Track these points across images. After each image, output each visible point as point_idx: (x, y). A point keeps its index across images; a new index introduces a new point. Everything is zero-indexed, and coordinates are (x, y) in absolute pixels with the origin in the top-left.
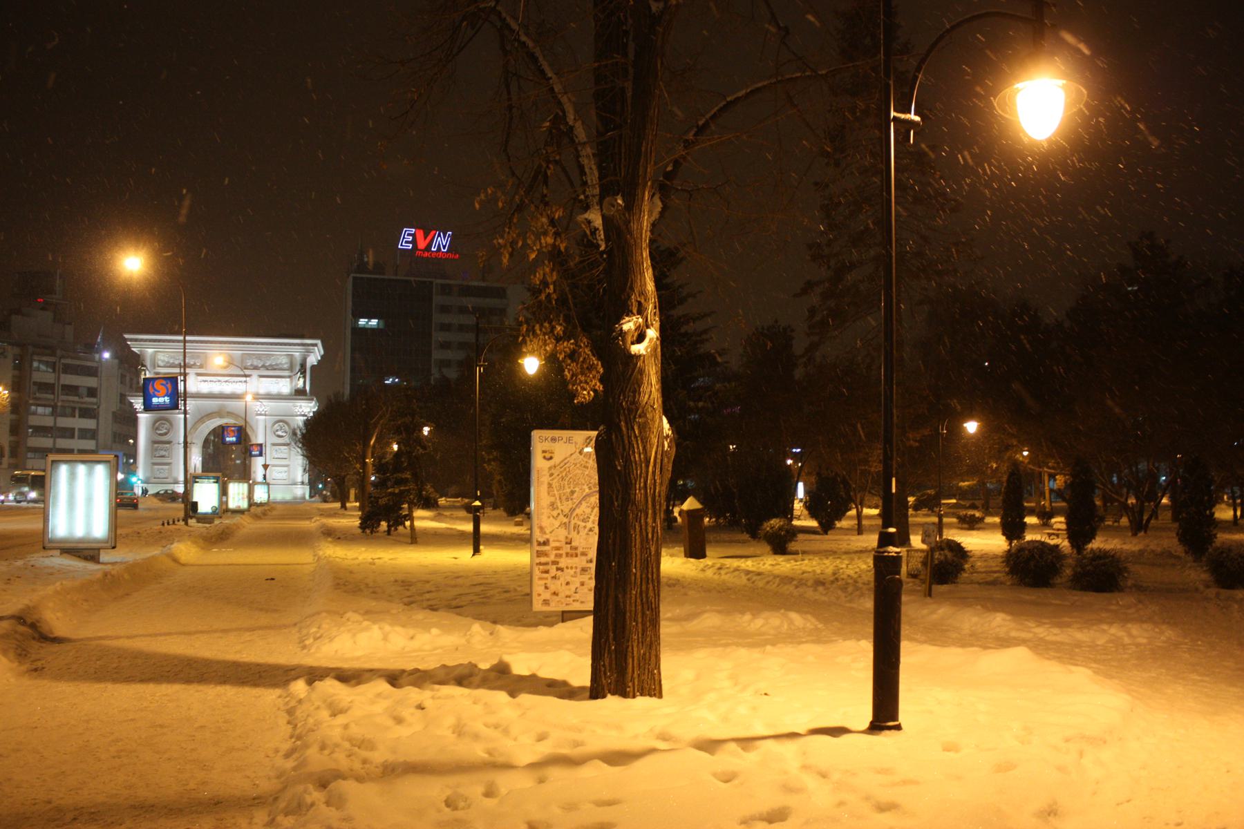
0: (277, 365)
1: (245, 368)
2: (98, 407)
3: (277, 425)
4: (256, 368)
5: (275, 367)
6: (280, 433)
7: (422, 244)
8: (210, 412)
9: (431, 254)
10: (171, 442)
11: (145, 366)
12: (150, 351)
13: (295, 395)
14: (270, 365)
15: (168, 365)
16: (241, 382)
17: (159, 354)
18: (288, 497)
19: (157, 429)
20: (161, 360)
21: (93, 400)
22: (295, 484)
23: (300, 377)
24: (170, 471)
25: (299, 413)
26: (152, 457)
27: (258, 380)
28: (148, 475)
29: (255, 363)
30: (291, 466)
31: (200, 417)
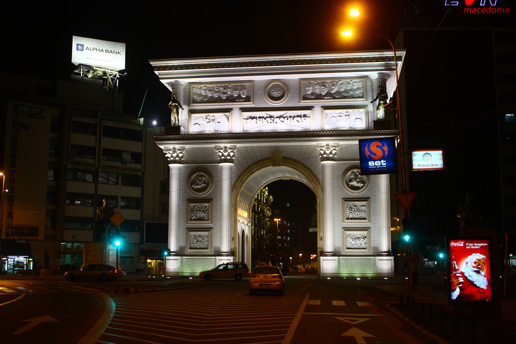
0: (346, 91)
1: (305, 98)
2: (143, 174)
3: (350, 173)
4: (319, 97)
5: (345, 95)
6: (354, 183)
8: (260, 158)
9: (480, 11)
10: (212, 199)
11: (177, 102)
12: (184, 82)
13: (375, 129)
14: (338, 93)
15: (207, 99)
16: (298, 116)
18: (370, 273)
19: (194, 183)
20: (197, 94)
21: (138, 166)
22: (380, 254)
24: (210, 238)
26: (187, 221)
27: (322, 112)
28: (183, 244)
29: (317, 91)
30: (372, 230)
31: (246, 166)
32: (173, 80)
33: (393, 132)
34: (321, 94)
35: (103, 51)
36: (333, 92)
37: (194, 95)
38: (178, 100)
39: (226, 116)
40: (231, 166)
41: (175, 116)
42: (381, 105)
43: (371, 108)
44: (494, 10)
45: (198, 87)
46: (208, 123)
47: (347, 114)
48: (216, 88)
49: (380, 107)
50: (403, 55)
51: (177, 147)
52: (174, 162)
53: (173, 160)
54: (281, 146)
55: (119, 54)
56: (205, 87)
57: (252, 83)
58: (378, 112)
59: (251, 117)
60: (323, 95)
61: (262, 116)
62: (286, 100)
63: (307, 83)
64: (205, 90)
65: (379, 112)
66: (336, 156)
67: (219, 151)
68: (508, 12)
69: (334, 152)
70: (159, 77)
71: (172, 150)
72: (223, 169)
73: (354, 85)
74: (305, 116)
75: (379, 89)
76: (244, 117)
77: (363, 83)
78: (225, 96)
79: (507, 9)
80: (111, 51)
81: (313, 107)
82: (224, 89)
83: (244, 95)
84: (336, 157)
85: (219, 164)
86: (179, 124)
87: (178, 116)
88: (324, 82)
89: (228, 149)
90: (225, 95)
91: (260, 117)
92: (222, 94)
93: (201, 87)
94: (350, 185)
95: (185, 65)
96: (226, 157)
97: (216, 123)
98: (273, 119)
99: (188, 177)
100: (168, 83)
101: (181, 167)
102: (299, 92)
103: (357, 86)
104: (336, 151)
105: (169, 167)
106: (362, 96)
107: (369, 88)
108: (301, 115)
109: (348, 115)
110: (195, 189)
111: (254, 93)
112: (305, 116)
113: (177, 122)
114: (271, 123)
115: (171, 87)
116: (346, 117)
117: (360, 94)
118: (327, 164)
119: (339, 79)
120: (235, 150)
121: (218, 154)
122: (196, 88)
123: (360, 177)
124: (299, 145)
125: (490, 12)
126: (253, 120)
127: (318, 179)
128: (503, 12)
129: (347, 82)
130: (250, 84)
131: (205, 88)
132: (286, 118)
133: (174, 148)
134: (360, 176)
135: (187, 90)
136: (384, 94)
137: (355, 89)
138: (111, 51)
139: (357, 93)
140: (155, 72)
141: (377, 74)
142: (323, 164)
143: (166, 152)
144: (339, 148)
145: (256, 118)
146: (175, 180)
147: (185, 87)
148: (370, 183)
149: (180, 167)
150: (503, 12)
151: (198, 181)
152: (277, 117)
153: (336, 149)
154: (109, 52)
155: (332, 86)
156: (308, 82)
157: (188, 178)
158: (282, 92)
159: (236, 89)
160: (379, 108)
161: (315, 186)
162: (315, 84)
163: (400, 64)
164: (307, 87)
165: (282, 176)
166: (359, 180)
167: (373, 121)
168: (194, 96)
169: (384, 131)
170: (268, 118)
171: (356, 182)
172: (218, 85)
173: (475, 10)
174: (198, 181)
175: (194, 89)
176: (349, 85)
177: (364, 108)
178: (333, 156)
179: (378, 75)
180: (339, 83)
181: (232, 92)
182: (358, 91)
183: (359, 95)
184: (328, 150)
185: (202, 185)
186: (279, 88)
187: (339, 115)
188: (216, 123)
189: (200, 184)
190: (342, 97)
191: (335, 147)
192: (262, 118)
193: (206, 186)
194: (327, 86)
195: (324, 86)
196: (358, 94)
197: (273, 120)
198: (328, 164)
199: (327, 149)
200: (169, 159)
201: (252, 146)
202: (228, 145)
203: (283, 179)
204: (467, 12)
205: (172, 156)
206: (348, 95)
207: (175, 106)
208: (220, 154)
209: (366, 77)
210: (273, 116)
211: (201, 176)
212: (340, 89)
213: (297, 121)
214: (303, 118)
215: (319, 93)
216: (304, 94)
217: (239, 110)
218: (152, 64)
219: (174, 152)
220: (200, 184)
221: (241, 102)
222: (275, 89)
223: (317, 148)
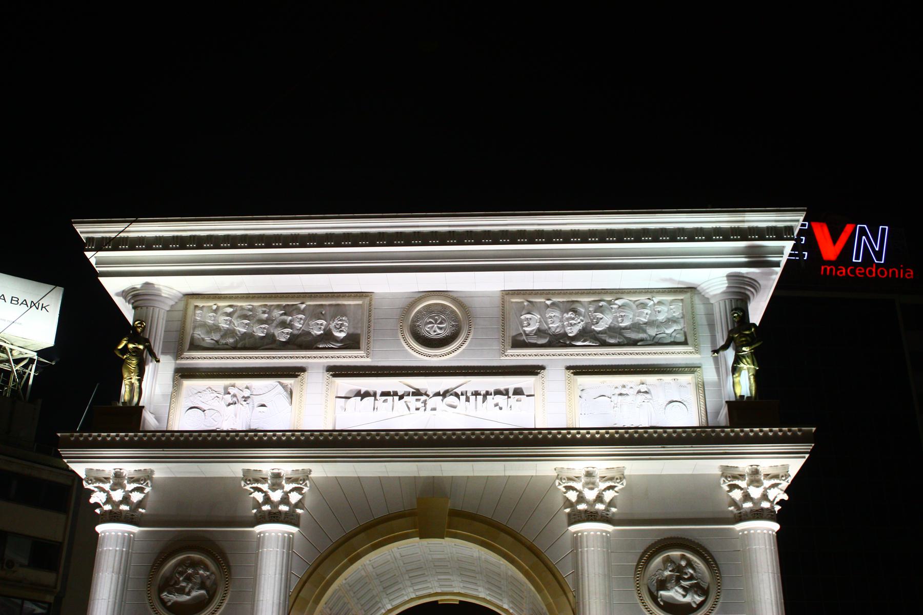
0: (636, 327)
1: (519, 343)
3: (658, 560)
4: (559, 341)
7: (829, 250)
9: (853, 272)
11: (145, 341)
14: (613, 330)
15: (231, 340)
16: (498, 392)
17: (200, 304)
19: (169, 584)
20: (204, 325)
21: (48, 577)
23: (738, 359)
25: (748, 505)
27: (569, 384)
29: (555, 326)
31: (337, 536)
32: (137, 282)
33: (789, 434)
34: (565, 335)
35: (4, 299)
36: (596, 329)
37: (195, 328)
38: (147, 337)
39: (284, 387)
40: (289, 533)
41: (133, 381)
42: (744, 361)
43: (709, 373)
44: (882, 273)
45: (211, 306)
46: (229, 405)
47: (643, 389)
48: (261, 312)
49: (742, 365)
50: (796, 223)
51: (129, 469)
52: (114, 517)
53: (110, 511)
54: (445, 477)
55: (43, 309)
56: (231, 306)
57: (368, 298)
58: (736, 380)
59: (360, 391)
60: (570, 335)
61: (391, 390)
62: (463, 347)
63: (526, 303)
64: (230, 315)
65: (736, 377)
66: (614, 510)
67: (255, 485)
68: (912, 277)
69: (608, 496)
70: (97, 269)
71: (112, 482)
72: (263, 543)
73: (659, 312)
74: (518, 392)
75: (735, 317)
76: (337, 392)
77: (682, 306)
78: (287, 333)
79: (909, 272)
80: (25, 300)
81: (543, 368)
82: (285, 314)
83: (342, 331)
84: (614, 514)
85: (253, 526)
86: (141, 404)
87: (140, 381)
88: (573, 302)
89: (284, 482)
90: (289, 330)
91: (384, 394)
92: (277, 326)
93: (218, 308)
94: (661, 600)
95: (177, 237)
96: (274, 505)
97: (253, 407)
98: (426, 400)
99: (153, 566)
100: (124, 294)
101: (133, 534)
102: (501, 327)
103: (667, 312)
104: (616, 492)
105: (98, 534)
106: (681, 338)
107: (702, 320)
108: (507, 391)
109: (646, 392)
110: (170, 604)
111: (372, 328)
112: (518, 392)
113: (136, 399)
114: (417, 409)
115: (133, 304)
116: (641, 397)
117: (677, 336)
118: (589, 531)
119: (617, 293)
120: (306, 485)
121: (252, 496)
122: (205, 309)
123: (692, 574)
124: (502, 474)
125: (874, 275)
126: (366, 399)
127: (561, 580)
128: (902, 276)
129: (637, 303)
130: (360, 302)
131: (230, 310)
132: (463, 398)
133: (118, 475)
134: (691, 571)
135: (178, 315)
136: (750, 329)
137: (662, 323)
138: (25, 300)
139: (669, 331)
140: (88, 254)
141: (725, 279)
142: (575, 533)
143: (91, 487)
144: (625, 484)
145: (375, 395)
146: (110, 576)
147: (172, 306)
148: (722, 595)
149: (130, 533)
150: (902, 276)
151: (181, 579)
152: (437, 394)
153: (615, 487)
154: (20, 302)
155: (595, 312)
156: (528, 301)
157: (152, 568)
158: (453, 326)
159: (320, 315)
160: (737, 369)
161: (552, 601)
162: (548, 306)
163: (788, 245)
164: (523, 313)
165: (439, 591)
166: (688, 583)
167: (729, 403)
168: (196, 330)
169: (761, 431)
170: (408, 395)
171: (680, 591)
172: (269, 304)
173: (844, 271)
174: (184, 580)
175: (198, 312)
176: (646, 311)
177: (693, 372)
178: (607, 510)
179: (729, 283)
180: (616, 304)
181: (308, 325)
182: (670, 327)
183: (675, 337)
184: (592, 489)
185: (194, 593)
186: (442, 313)
187: (618, 391)
188: (253, 407)
189: (187, 590)
190: (626, 342)
191: (611, 479)
192: (393, 396)
193: (207, 597)
194: (583, 313)
195: (575, 311)
196: (671, 335)
197: (425, 402)
198: (592, 533)
199: (591, 486)
200: (98, 511)
201: (358, 477)
202: (287, 469)
203: (441, 600)
204: (828, 273)
205: (109, 500)
206: (641, 336)
207: (134, 352)
208: (259, 497)
209: (691, 289)
210: (423, 392)
211: (195, 564)
212: (618, 322)
213: (496, 405)
214: (514, 398)
215: (558, 330)
216: (514, 334)
217: (326, 373)
218: (81, 232)
219: (116, 487)
220: (187, 590)
221: (332, 348)
222: (432, 318)
223: (557, 482)
